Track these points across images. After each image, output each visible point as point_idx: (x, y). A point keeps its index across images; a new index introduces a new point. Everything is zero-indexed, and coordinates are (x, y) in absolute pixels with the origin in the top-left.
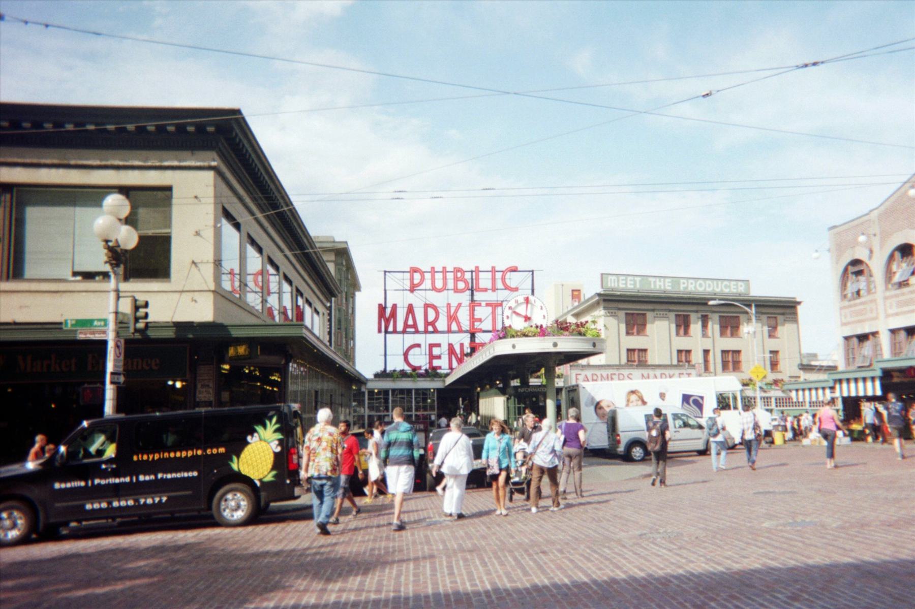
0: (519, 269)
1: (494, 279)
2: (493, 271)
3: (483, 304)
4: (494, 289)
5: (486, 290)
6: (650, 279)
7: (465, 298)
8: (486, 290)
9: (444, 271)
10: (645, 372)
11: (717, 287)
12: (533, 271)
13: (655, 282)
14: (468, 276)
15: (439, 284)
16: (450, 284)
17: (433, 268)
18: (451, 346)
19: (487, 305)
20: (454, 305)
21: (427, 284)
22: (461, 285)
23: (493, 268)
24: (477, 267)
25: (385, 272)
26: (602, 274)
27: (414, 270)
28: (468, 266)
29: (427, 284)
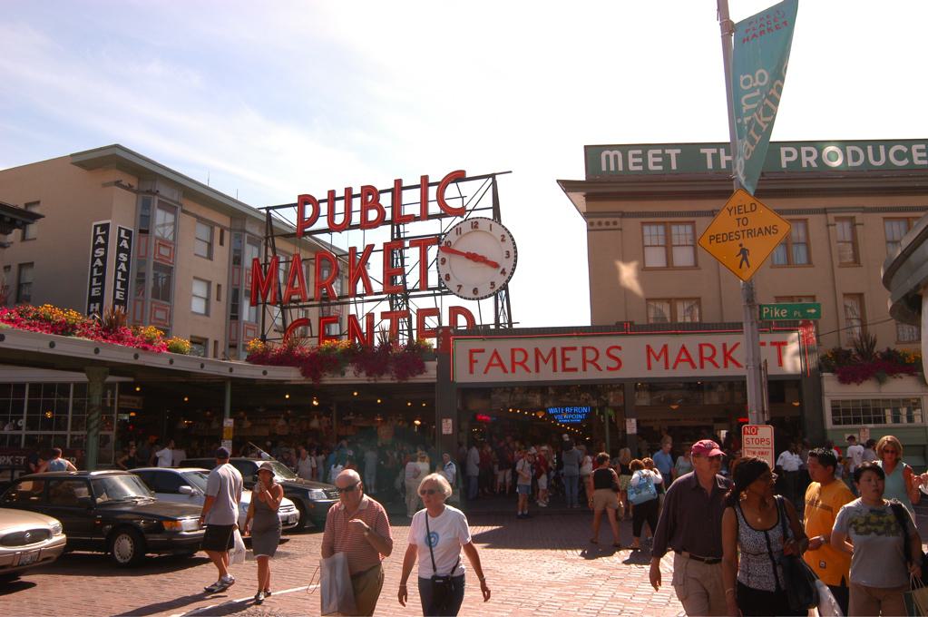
0: (468, 176)
1: (424, 202)
2: (425, 183)
3: (407, 244)
4: (425, 216)
5: (412, 218)
6: (703, 151)
7: (382, 235)
8: (412, 218)
9: (349, 195)
10: (657, 342)
11: (877, 158)
12: (493, 176)
13: (716, 157)
14: (386, 200)
15: (339, 220)
16: (356, 219)
17: (332, 193)
18: (353, 318)
19: (413, 245)
20: (360, 249)
21: (322, 223)
22: (373, 215)
23: (424, 179)
24: (398, 182)
25: (268, 209)
26: (585, 147)
27: (305, 200)
28: (384, 182)
29: (322, 223)
